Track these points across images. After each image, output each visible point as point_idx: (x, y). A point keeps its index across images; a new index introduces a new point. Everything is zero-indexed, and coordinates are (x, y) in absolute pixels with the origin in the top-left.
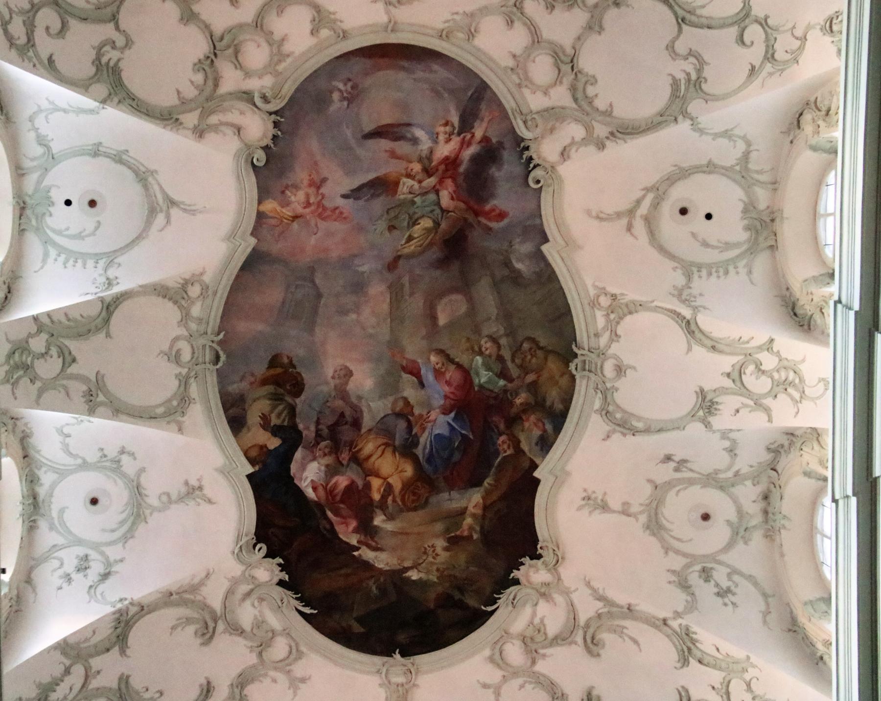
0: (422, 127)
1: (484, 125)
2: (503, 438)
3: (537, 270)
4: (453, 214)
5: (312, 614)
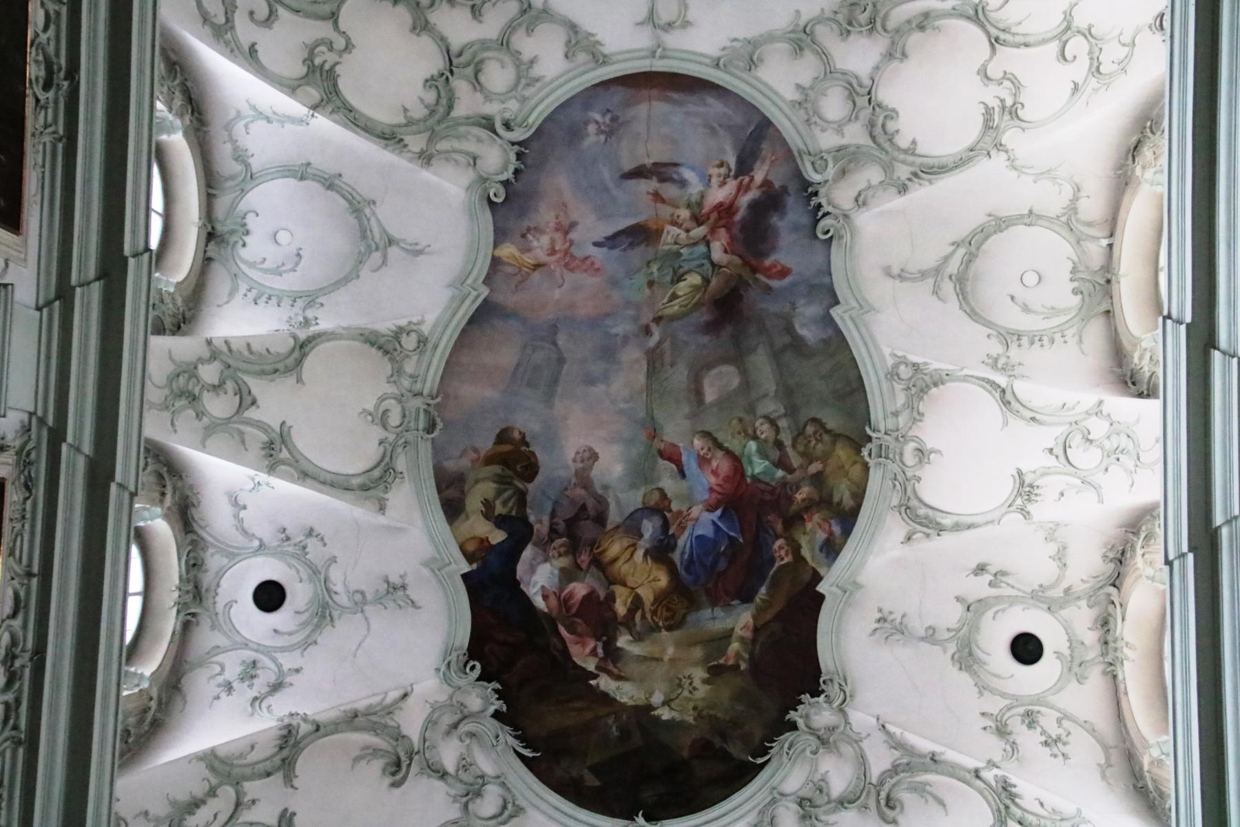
0: (693, 169)
1: (766, 168)
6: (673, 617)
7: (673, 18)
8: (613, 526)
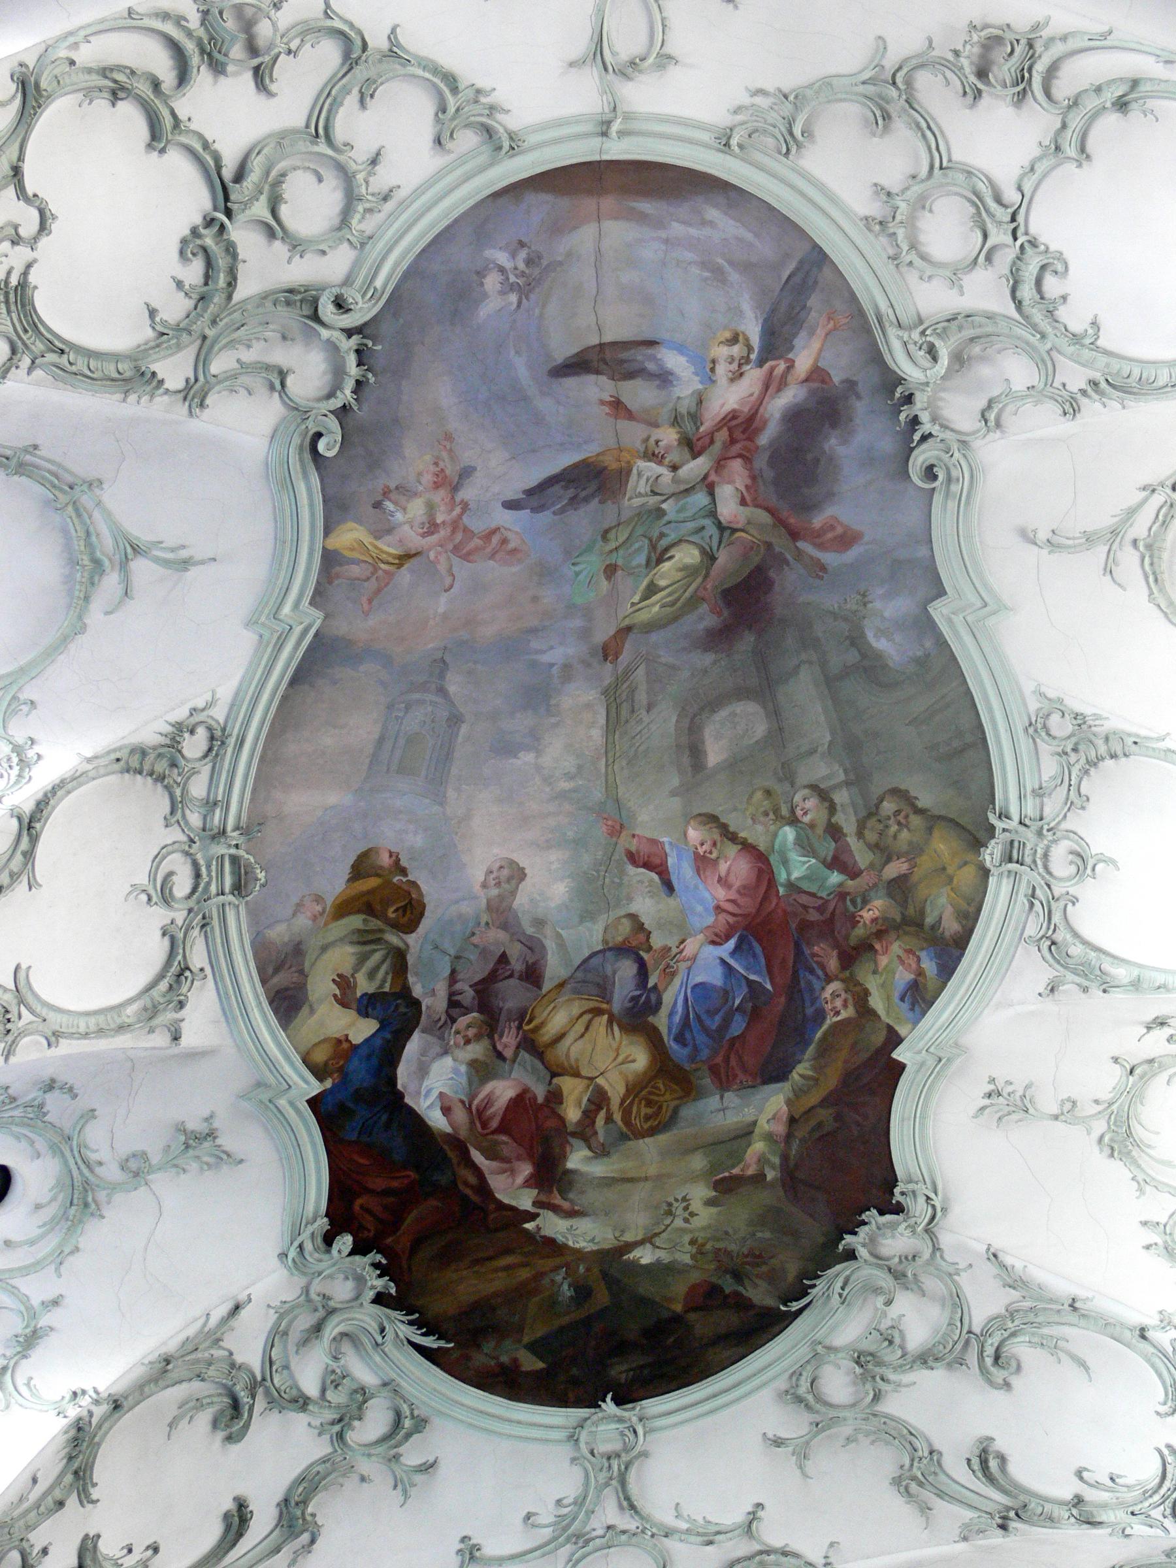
0: (681, 349)
1: (816, 344)
2: (835, 986)
3: (919, 653)
4: (743, 534)
5: (439, 1348)
6: (656, 1114)
8: (556, 982)
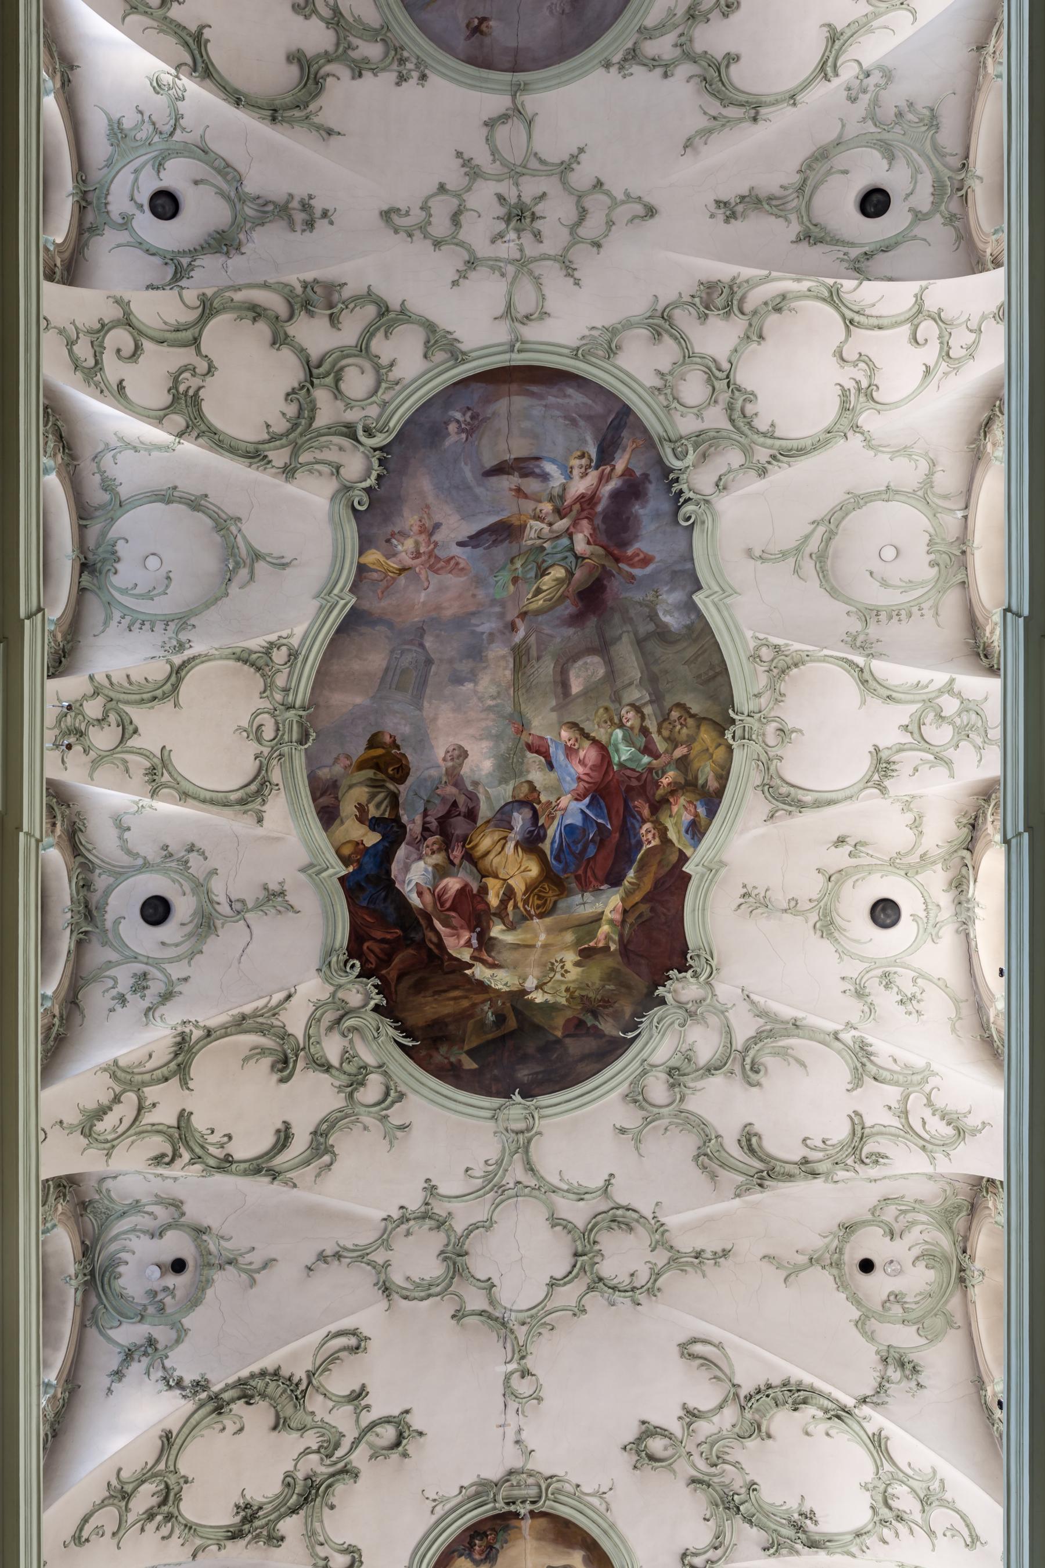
0: (553, 461)
1: (626, 456)
2: (647, 826)
7: (531, 311)
